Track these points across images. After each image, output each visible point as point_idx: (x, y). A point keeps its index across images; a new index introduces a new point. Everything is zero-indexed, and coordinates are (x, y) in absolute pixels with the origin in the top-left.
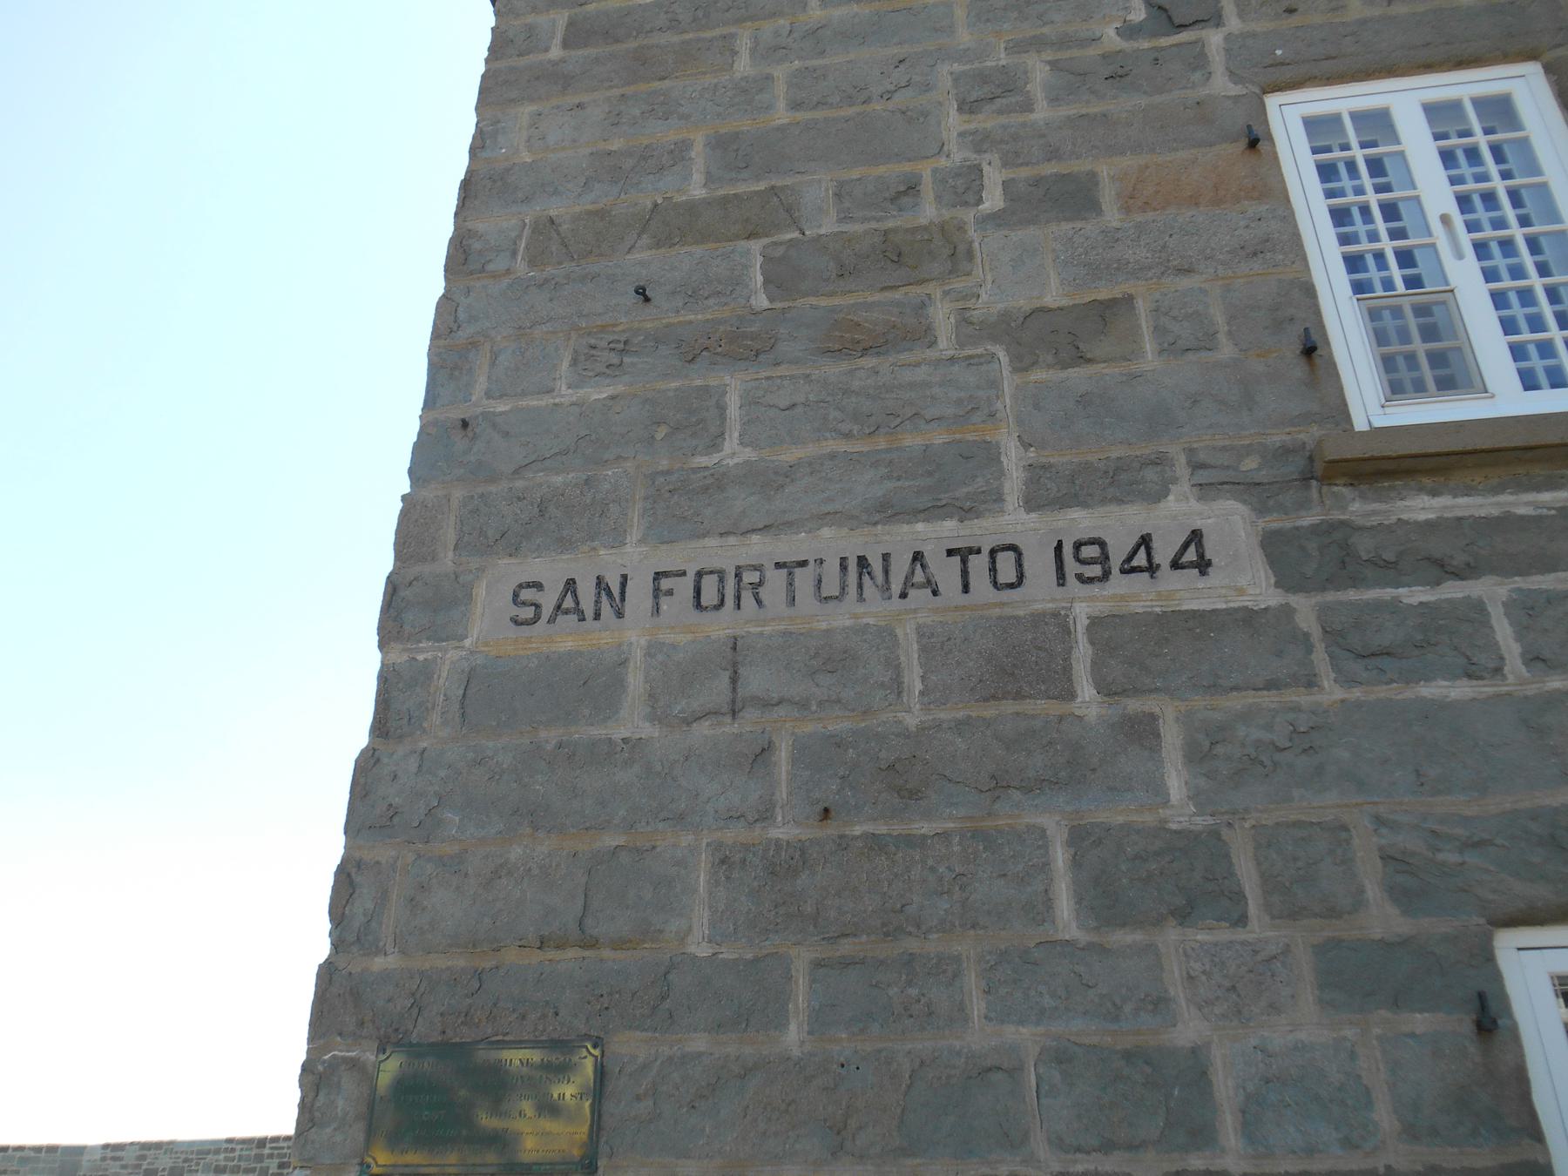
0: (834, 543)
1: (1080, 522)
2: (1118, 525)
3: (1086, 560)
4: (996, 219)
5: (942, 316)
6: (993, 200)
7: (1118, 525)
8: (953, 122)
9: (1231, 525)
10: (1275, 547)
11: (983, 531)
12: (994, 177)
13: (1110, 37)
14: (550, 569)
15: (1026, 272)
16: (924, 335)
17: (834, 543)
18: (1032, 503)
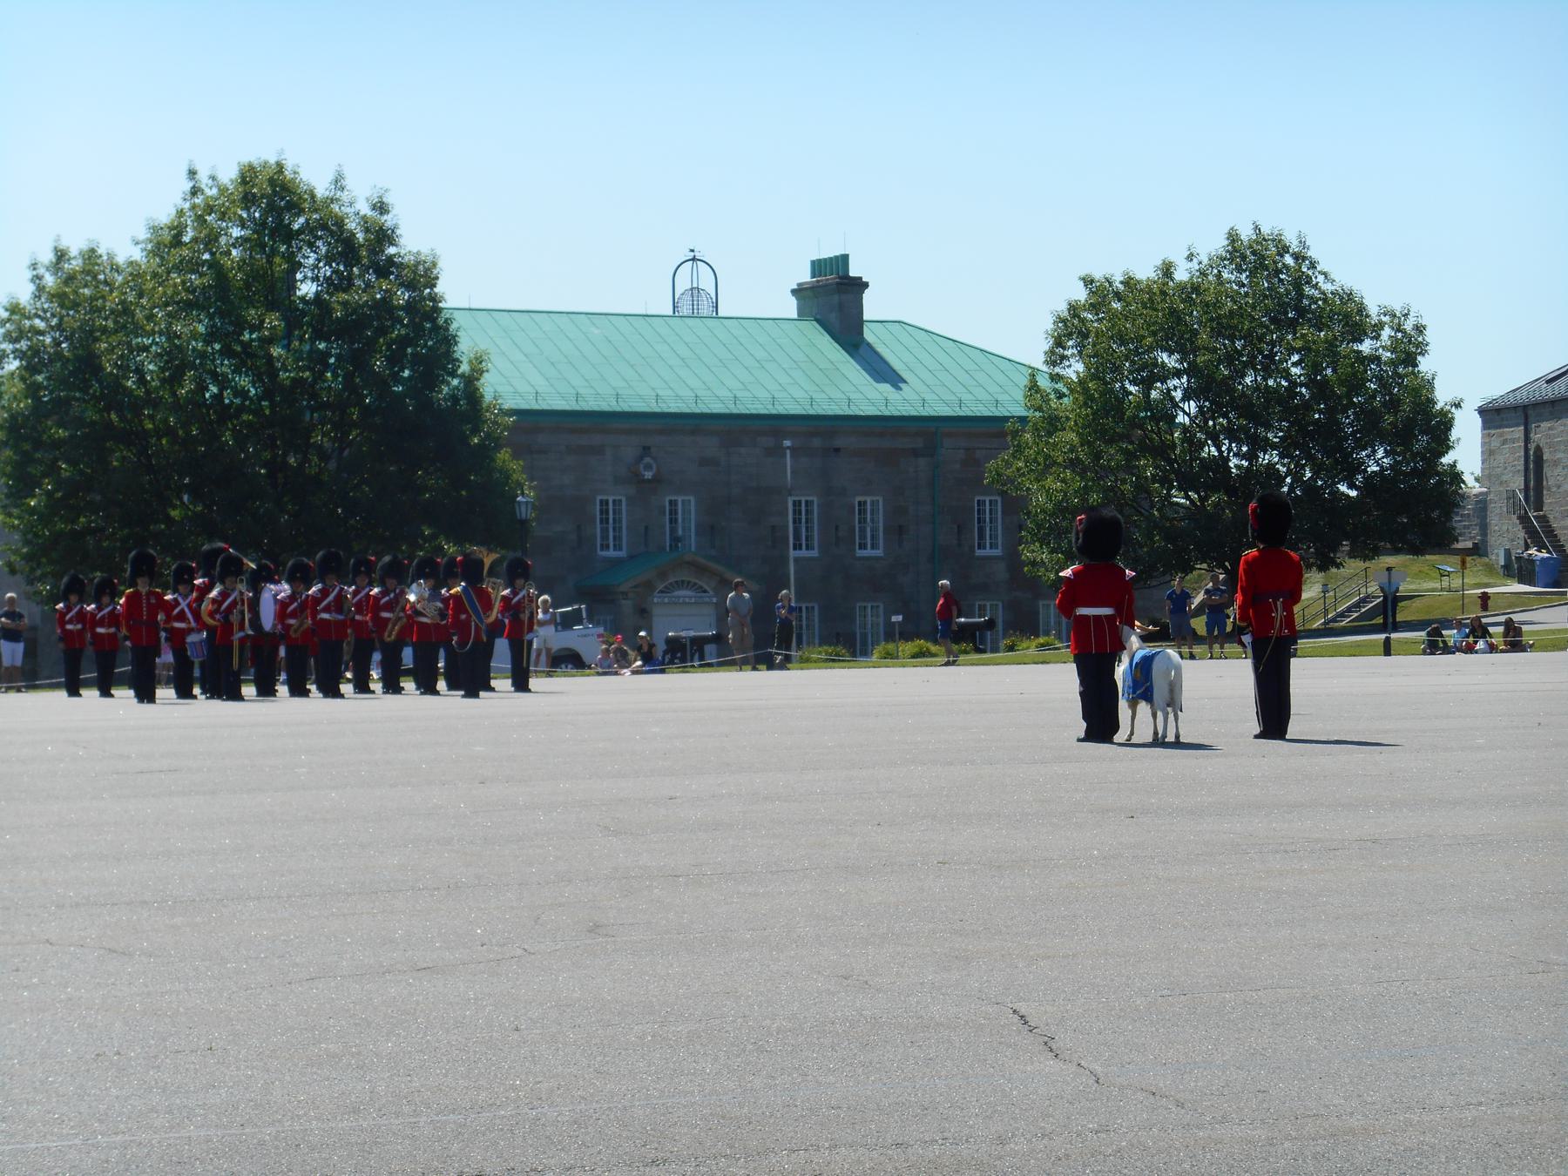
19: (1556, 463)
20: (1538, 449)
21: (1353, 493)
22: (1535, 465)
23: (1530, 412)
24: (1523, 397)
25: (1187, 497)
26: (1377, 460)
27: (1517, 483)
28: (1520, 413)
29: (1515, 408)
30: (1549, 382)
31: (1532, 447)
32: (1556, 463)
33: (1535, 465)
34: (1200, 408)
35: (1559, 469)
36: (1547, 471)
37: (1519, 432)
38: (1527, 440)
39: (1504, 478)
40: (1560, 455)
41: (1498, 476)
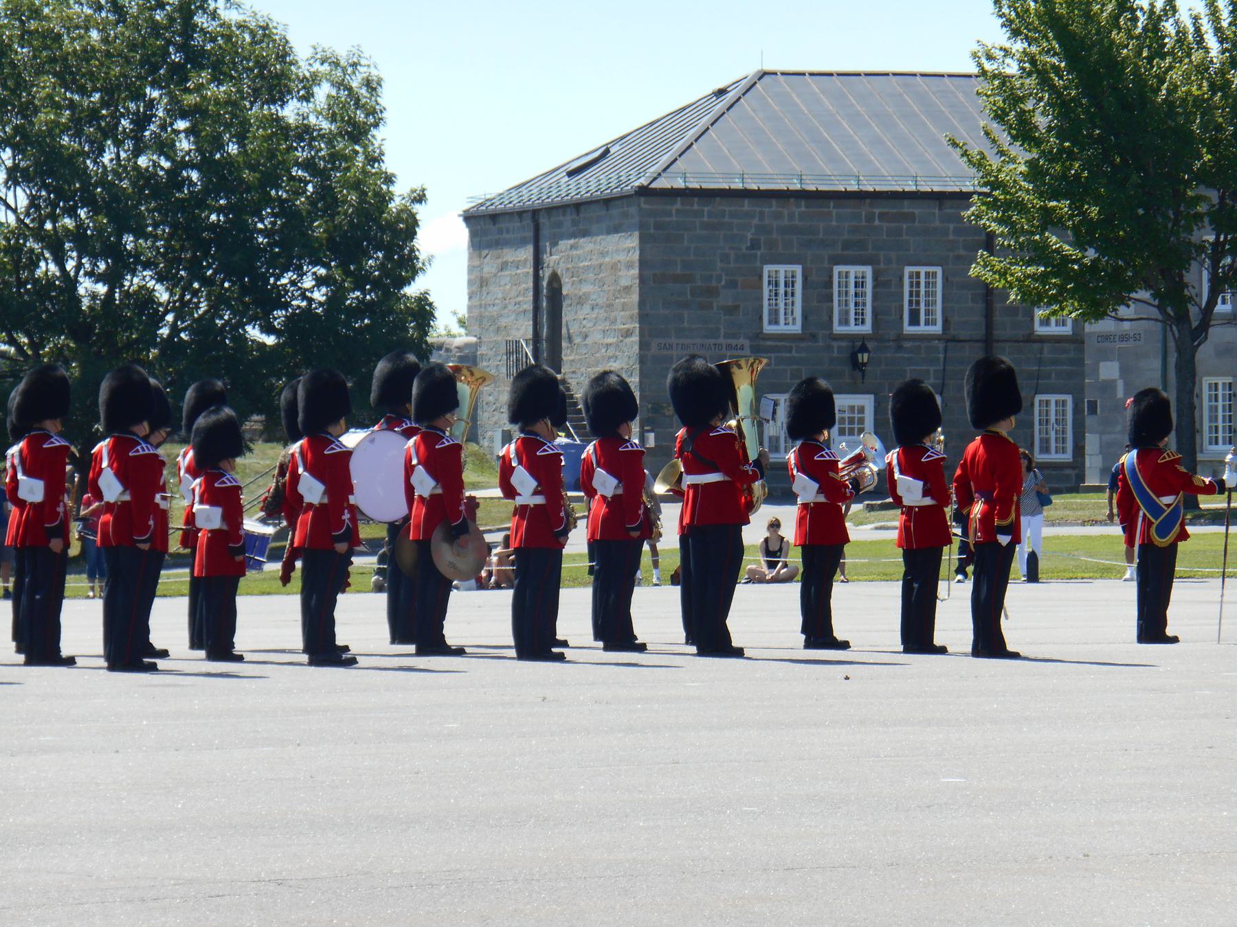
0: (699, 341)
1: (729, 341)
2: (734, 342)
3: (729, 347)
4: (724, 287)
5: (715, 305)
6: (723, 283)
7: (734, 342)
8: (719, 264)
9: (747, 343)
10: (751, 347)
11: (718, 341)
12: (724, 278)
13: (744, 251)
14: (662, 341)
15: (725, 298)
16: (710, 307)
17: (699, 341)
18: (725, 338)
19: (581, 301)
20: (555, 278)
21: (270, 340)
22: (549, 301)
23: (543, 220)
24: (532, 198)
25: (12, 341)
26: (308, 286)
27: (523, 330)
28: (528, 221)
29: (520, 214)
30: (571, 174)
31: (546, 274)
32: (581, 301)
33: (549, 301)
34: (33, 202)
35: (586, 309)
36: (567, 315)
37: (527, 253)
38: (538, 263)
39: (503, 322)
40: (586, 288)
41: (493, 320)
